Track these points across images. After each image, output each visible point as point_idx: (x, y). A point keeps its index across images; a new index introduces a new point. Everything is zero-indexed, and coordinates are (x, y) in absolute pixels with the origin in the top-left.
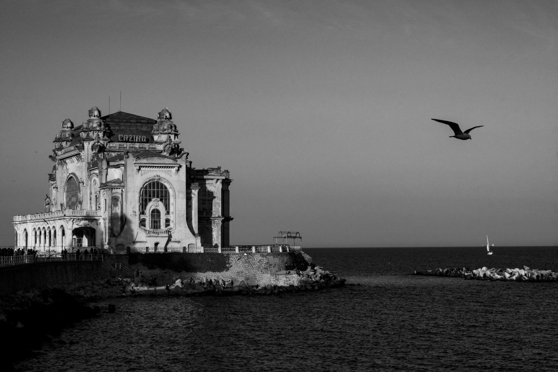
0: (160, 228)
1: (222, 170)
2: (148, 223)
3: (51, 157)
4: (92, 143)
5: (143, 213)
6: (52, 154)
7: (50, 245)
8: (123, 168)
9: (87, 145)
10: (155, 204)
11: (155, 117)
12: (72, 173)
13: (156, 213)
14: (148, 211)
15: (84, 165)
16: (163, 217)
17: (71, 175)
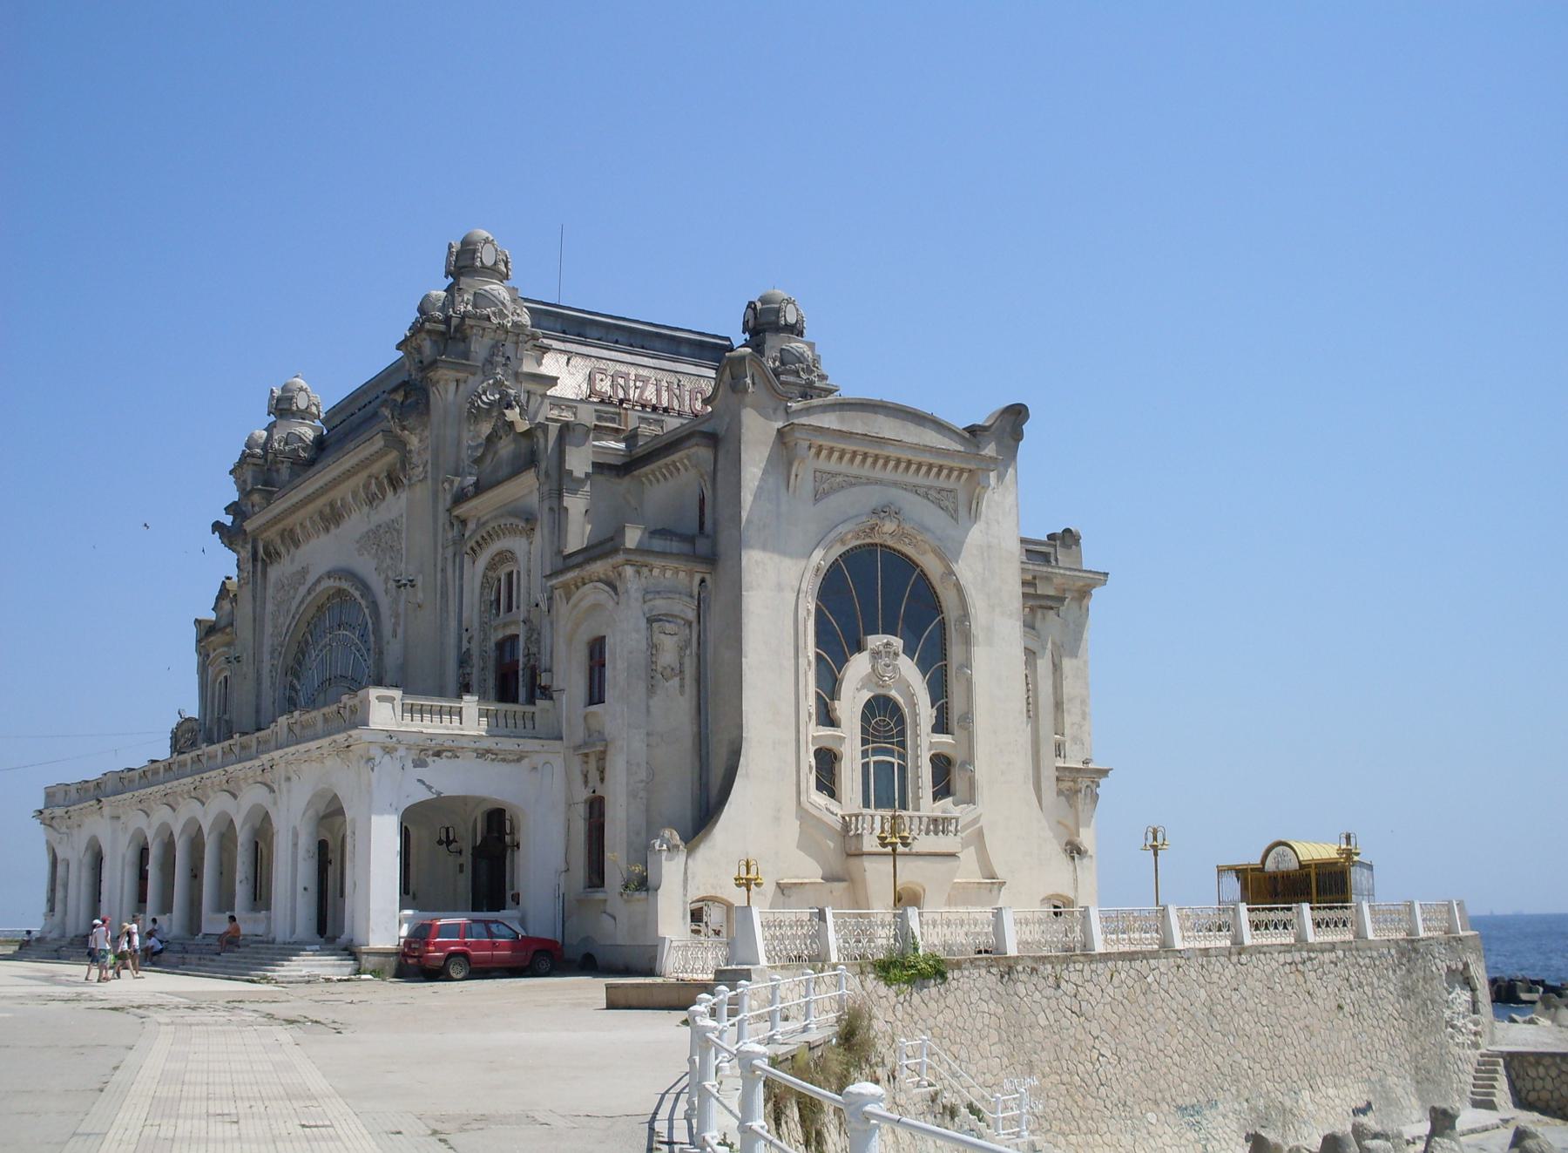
0: (904, 806)
3: (217, 526)
5: (827, 717)
6: (228, 520)
7: (225, 902)
8: (703, 453)
10: (883, 665)
12: (329, 575)
16: (925, 741)
17: (331, 583)
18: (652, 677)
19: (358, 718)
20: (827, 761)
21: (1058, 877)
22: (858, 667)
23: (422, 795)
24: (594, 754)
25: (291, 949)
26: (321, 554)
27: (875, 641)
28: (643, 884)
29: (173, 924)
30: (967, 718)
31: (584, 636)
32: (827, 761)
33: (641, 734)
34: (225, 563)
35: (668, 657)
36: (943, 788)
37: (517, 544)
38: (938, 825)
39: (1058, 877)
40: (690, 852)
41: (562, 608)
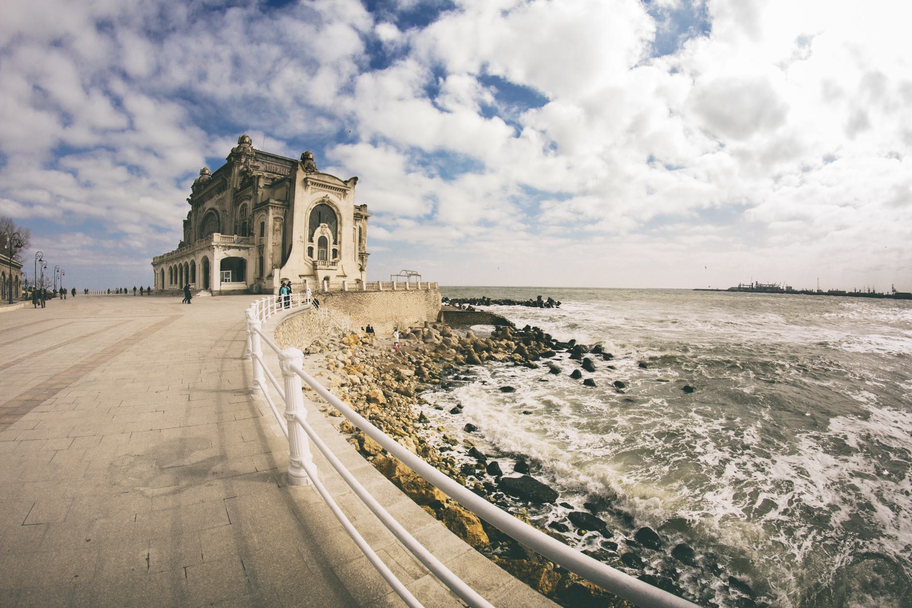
4: (241, 167)
10: (324, 230)
13: (323, 242)
14: (316, 238)
15: (228, 195)
18: (275, 231)
19: (211, 239)
20: (311, 250)
21: (358, 275)
22: (319, 229)
23: (225, 257)
24: (261, 248)
25: (200, 291)
26: (209, 205)
27: (322, 224)
28: (271, 276)
30: (340, 242)
31: (259, 223)
32: (311, 250)
34: (189, 208)
35: (277, 227)
36: (335, 256)
37: (247, 202)
38: (334, 264)
39: (358, 275)
40: (281, 268)
41: (256, 216)
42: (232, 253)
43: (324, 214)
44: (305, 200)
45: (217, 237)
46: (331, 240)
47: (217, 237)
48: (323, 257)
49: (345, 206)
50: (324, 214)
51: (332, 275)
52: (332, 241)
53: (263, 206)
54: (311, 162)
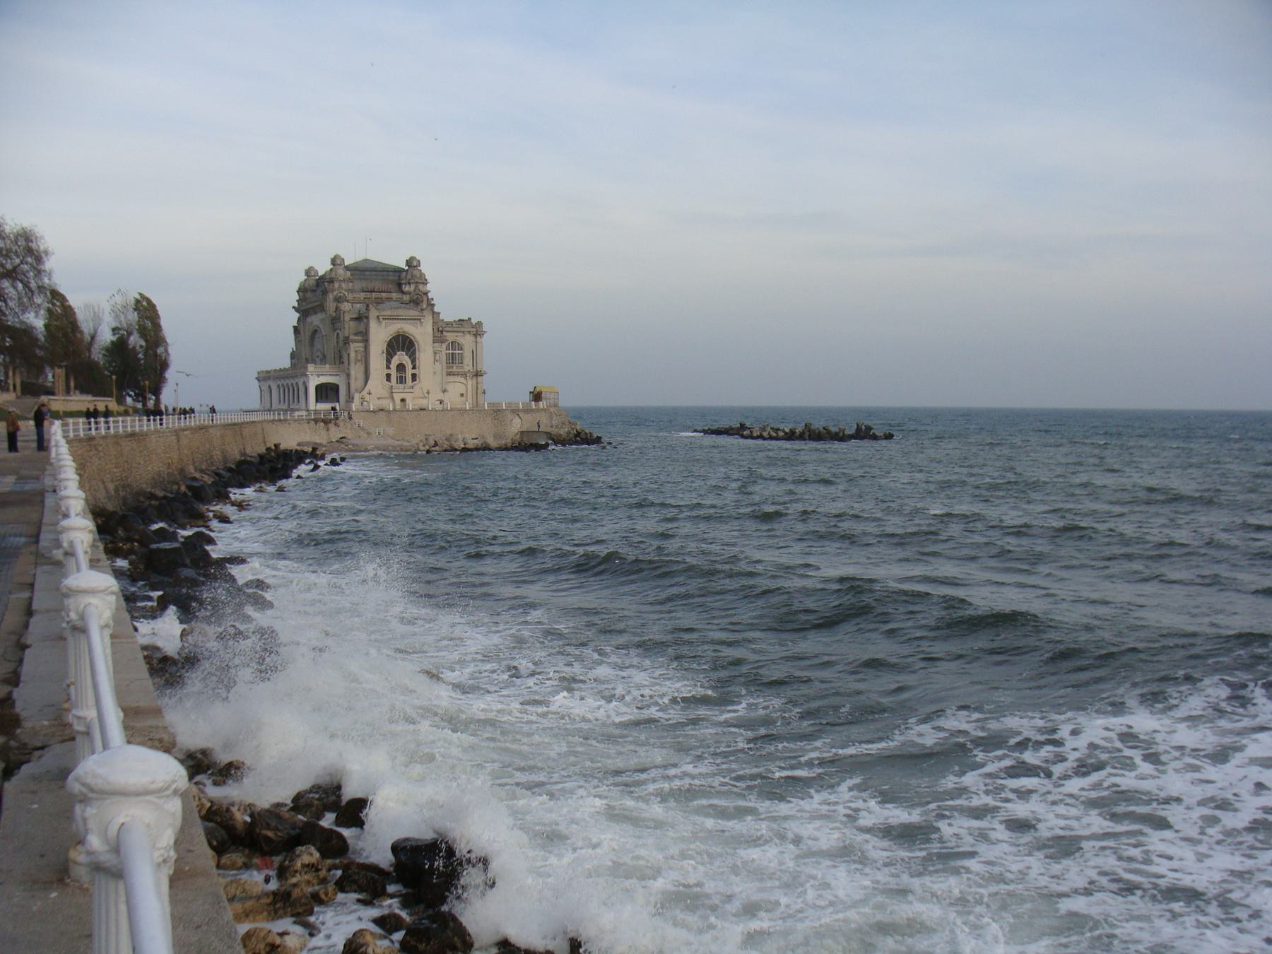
1: (474, 321)
2: (393, 378)
6: (296, 304)
9: (331, 296)
10: (401, 357)
11: (403, 265)
13: (401, 367)
19: (306, 368)
20: (388, 377)
24: (348, 375)
26: (315, 320)
29: (268, 406)
32: (388, 377)
33: (356, 371)
39: (441, 396)
42: (324, 380)
43: (402, 343)
44: (380, 335)
45: (311, 367)
46: (409, 365)
47: (311, 367)
48: (401, 380)
49: (422, 333)
50: (402, 343)
51: (408, 397)
52: (411, 366)
53: (347, 341)
54: (416, 272)
